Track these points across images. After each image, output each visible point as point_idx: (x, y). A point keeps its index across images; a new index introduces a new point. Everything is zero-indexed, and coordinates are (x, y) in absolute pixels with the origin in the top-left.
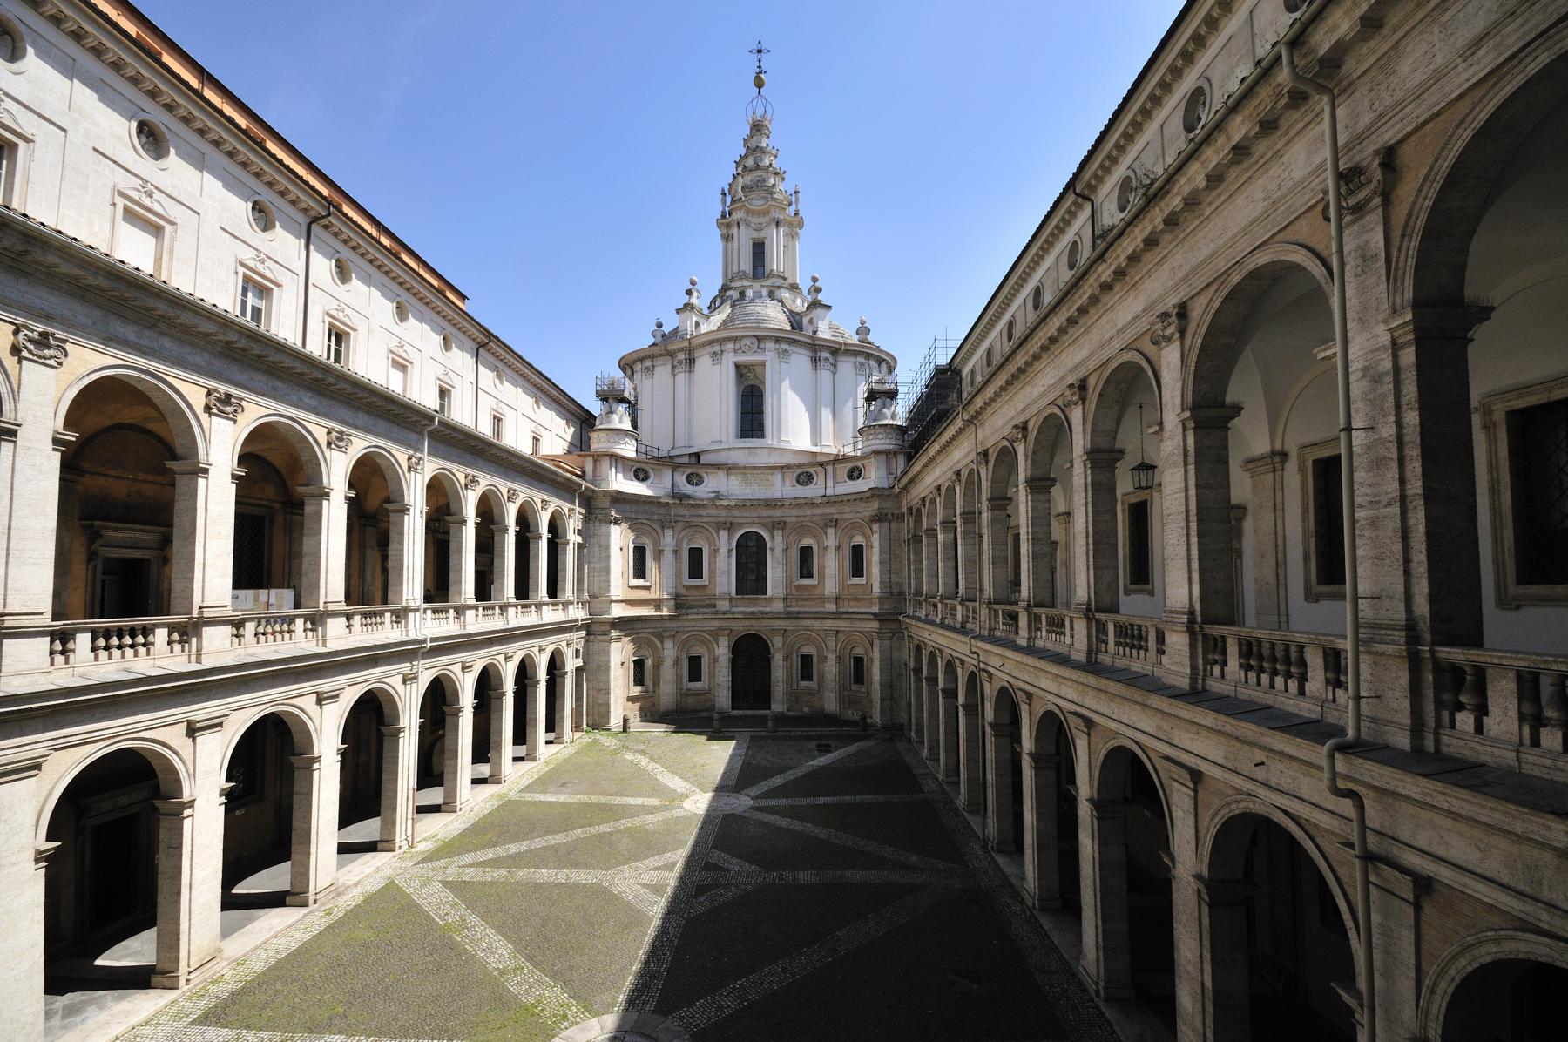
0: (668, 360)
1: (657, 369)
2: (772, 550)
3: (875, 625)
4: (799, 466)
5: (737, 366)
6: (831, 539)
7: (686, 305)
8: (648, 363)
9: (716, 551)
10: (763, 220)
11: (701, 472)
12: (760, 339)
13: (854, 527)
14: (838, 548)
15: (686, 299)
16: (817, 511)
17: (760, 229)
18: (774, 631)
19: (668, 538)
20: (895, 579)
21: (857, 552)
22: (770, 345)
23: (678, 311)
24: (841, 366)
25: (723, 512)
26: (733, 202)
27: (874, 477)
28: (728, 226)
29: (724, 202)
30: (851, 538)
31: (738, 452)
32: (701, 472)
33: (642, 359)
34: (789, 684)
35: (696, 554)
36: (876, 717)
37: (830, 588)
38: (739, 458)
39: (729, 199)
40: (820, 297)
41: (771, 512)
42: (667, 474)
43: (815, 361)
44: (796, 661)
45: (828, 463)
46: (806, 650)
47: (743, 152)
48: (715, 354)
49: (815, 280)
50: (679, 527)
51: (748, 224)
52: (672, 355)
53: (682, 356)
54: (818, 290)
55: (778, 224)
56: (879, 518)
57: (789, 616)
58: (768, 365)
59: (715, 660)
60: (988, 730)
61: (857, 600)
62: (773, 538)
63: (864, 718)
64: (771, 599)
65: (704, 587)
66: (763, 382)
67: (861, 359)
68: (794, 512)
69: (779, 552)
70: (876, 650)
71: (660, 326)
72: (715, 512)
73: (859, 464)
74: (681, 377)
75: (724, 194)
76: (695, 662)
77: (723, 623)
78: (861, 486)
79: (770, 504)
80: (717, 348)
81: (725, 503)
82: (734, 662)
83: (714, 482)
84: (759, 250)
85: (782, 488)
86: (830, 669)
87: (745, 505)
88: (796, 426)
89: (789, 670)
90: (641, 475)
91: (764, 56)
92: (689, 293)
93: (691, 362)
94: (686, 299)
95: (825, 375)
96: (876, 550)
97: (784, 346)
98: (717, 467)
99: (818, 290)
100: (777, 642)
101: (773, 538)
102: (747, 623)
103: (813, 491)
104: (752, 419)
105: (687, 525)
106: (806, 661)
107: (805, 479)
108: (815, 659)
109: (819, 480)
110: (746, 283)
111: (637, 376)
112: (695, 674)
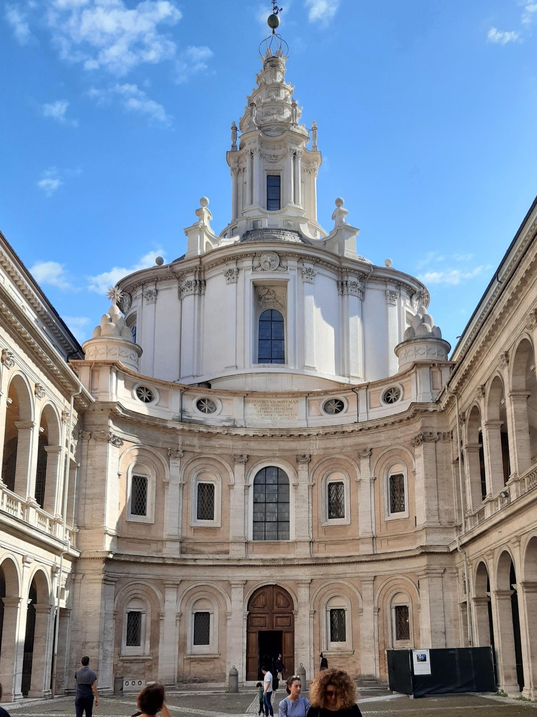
1: (160, 293)
2: (296, 486)
3: (423, 562)
4: (326, 393)
5: (256, 286)
6: (365, 470)
7: (195, 226)
9: (231, 487)
12: (282, 256)
13: (392, 454)
16: (349, 441)
20: (444, 506)
22: (292, 263)
27: (416, 392)
31: (256, 379)
32: (213, 398)
33: (143, 284)
34: (317, 644)
35: (206, 492)
38: (257, 384)
41: (293, 445)
45: (360, 387)
48: (230, 271)
50: (188, 456)
53: (191, 278)
56: (423, 439)
57: (317, 563)
58: (290, 285)
61: (398, 537)
65: (214, 530)
69: (303, 488)
70: (424, 592)
72: (229, 443)
73: (396, 384)
74: (189, 300)
78: (400, 407)
79: (289, 435)
80: (233, 266)
81: (242, 432)
82: (249, 618)
83: (227, 411)
88: (326, 344)
89: (316, 627)
93: (201, 284)
100: (302, 596)
111: (137, 303)
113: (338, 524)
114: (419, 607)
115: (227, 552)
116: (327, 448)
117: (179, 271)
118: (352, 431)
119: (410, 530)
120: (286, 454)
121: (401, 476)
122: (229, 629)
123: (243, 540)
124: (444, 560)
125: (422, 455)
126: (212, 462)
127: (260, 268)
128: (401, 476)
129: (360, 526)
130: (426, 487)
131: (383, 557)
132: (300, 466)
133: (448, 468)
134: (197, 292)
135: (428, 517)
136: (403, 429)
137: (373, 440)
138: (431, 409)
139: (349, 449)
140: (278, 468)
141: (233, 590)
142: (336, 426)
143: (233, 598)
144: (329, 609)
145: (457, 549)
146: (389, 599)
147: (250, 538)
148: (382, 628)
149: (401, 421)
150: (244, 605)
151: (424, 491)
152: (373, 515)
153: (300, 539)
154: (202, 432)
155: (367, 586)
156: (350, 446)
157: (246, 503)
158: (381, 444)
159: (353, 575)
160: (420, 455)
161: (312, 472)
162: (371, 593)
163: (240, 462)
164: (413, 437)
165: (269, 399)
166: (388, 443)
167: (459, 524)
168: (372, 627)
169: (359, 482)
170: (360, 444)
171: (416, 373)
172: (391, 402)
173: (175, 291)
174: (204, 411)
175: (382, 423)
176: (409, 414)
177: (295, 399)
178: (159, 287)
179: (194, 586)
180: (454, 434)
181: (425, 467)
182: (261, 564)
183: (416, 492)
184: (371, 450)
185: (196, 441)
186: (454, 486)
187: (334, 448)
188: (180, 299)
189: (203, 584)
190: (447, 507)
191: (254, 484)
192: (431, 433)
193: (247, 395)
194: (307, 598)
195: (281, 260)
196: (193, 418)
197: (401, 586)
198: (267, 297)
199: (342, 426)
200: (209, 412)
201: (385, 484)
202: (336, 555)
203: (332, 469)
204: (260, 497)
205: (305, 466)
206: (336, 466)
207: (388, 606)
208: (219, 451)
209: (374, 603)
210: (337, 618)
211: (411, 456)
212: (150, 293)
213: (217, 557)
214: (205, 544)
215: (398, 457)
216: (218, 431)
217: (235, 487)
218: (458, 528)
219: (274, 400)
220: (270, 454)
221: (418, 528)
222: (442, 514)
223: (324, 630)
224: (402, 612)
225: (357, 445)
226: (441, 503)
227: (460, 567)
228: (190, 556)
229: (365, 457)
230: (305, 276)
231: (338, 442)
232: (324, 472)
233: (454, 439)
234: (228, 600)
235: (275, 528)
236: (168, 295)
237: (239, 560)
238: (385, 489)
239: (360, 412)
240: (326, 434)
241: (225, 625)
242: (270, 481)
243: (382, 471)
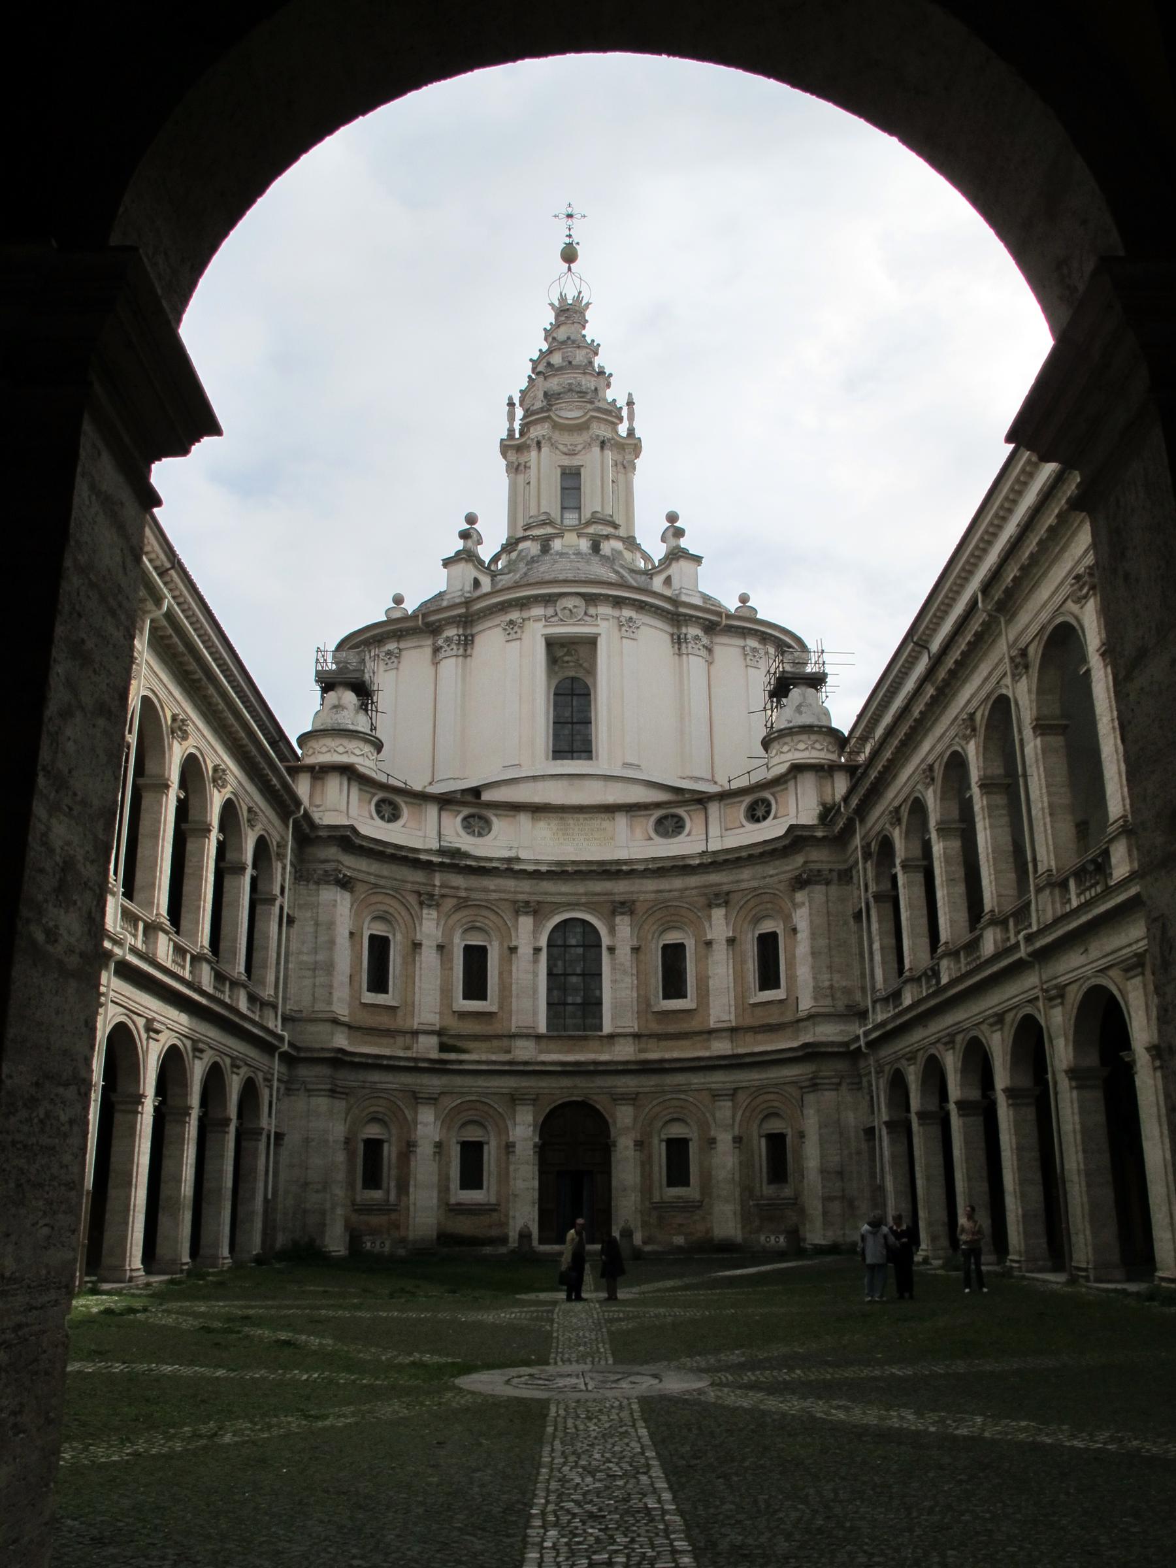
0: (429, 642)
1: (404, 653)
2: (611, 950)
4: (658, 805)
5: (552, 644)
6: (719, 926)
8: (392, 646)
9: (513, 950)
10: (579, 439)
11: (490, 814)
12: (591, 599)
13: (763, 903)
14: (731, 941)
15: (460, 545)
16: (693, 881)
17: (572, 454)
18: (618, 1099)
19: (430, 927)
20: (840, 982)
21: (768, 945)
22: (604, 610)
23: (447, 563)
24: (718, 650)
25: (526, 886)
26: (528, 413)
28: (520, 448)
29: (511, 417)
30: (757, 920)
34: (646, 1189)
35: (476, 958)
36: (816, 1235)
37: (721, 1009)
39: (519, 413)
40: (684, 543)
42: (432, 811)
43: (678, 641)
44: (660, 1152)
46: (677, 1131)
47: (545, 347)
48: (511, 622)
49: (672, 518)
50: (449, 903)
51: (554, 446)
52: (433, 630)
54: (679, 533)
55: (603, 444)
59: (509, 1147)
60: (1064, 1083)
62: (612, 930)
63: (794, 1235)
64: (611, 1037)
65: (490, 1015)
66: (592, 671)
67: (752, 643)
68: (651, 885)
69: (624, 952)
71: (398, 600)
72: (510, 884)
73: (767, 795)
75: (511, 404)
76: (472, 1154)
77: (524, 1083)
78: (772, 829)
80: (515, 615)
81: (531, 868)
82: (543, 1151)
84: (571, 479)
85: (631, 842)
86: (725, 1161)
87: (561, 872)
89: (646, 1164)
90: (388, 809)
91: (576, 222)
92: (465, 535)
93: (467, 642)
94: (460, 545)
95: (695, 663)
96: (803, 935)
97: (627, 613)
98: (515, 808)
99: (679, 533)
100: (623, 1117)
101: (612, 930)
102: (566, 1082)
103: (688, 844)
104: (572, 729)
105: (463, 904)
106: (678, 1149)
107: (670, 825)
108: (693, 1148)
109: (693, 823)
110: (549, 530)
112: (472, 1176)
113: (678, 1008)
114: (802, 1135)
115: (509, 1052)
116: (661, 891)
117: (433, 623)
118: (699, 865)
119: (789, 1017)
120: (595, 899)
121: (773, 936)
122: (512, 1168)
123: (530, 1031)
124: (841, 1066)
125: (807, 904)
126: (485, 912)
127: (556, 619)
128: (773, 936)
129: (712, 1011)
130: (813, 954)
131: (748, 1060)
132: (618, 919)
133: (846, 923)
134: (461, 651)
135: (815, 999)
136: (777, 863)
137: (731, 878)
138: (819, 834)
139: (694, 892)
140: (584, 922)
141: (518, 1108)
142: (674, 858)
143: (518, 1119)
144: (664, 1137)
145: (860, 1047)
146: (757, 1122)
147: (542, 1028)
148: (746, 1165)
149: (774, 850)
150: (534, 1131)
151: (810, 959)
152: (732, 994)
153: (619, 1030)
154: (470, 866)
155: (722, 1103)
156: (696, 888)
157: (536, 975)
158: (744, 886)
159: (701, 1087)
160: (803, 904)
161: (637, 927)
162: (729, 1113)
163: (527, 913)
164: (789, 875)
165: (569, 816)
166: (754, 884)
167: (862, 1006)
168: (730, 1165)
169: (709, 944)
170: (712, 885)
171: (795, 778)
172: (758, 821)
173: (428, 651)
174: (472, 833)
175: (744, 854)
176: (786, 842)
177: (609, 815)
178: (402, 645)
179: (459, 1101)
180: (854, 872)
181: (811, 921)
182: (559, 1069)
183: (798, 960)
184: (728, 893)
185: (458, 881)
186: (855, 950)
187: (670, 891)
188: (436, 664)
189: (474, 1098)
190: (844, 984)
191: (549, 946)
192: (819, 871)
193: (538, 810)
194: (628, 1121)
195: (587, 605)
196: (457, 845)
197: (776, 1104)
198: (566, 658)
199: (683, 857)
200: (480, 835)
201: (749, 946)
202: (676, 1055)
203: (668, 922)
204: (556, 965)
205: (627, 919)
206: (673, 918)
207: (755, 1134)
208: (494, 896)
209: (733, 1129)
210: (678, 1149)
211: (789, 904)
212: (389, 653)
213: (494, 1058)
214: (476, 1038)
215: (769, 906)
216: (494, 865)
217: (520, 951)
218: (862, 1015)
219: (576, 816)
220: (573, 899)
221: (801, 1014)
222: (838, 995)
223: (656, 1168)
224: (776, 1142)
225: (706, 887)
226: (836, 977)
227: (866, 1075)
228: (453, 1056)
229: (718, 906)
230: (624, 629)
231: (678, 883)
232: (655, 927)
233: (855, 880)
234: (509, 1123)
235: (579, 1013)
236: (416, 657)
237: (526, 1063)
238: (750, 954)
239: (711, 834)
240: (659, 869)
241: (508, 1163)
242: (573, 942)
243: (745, 926)
